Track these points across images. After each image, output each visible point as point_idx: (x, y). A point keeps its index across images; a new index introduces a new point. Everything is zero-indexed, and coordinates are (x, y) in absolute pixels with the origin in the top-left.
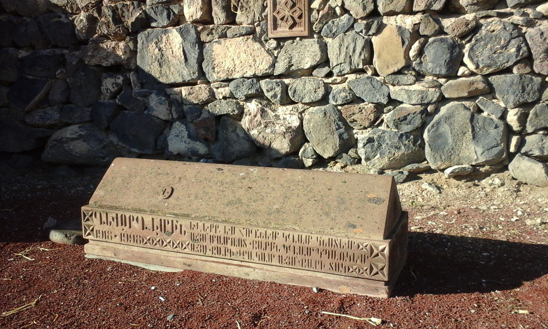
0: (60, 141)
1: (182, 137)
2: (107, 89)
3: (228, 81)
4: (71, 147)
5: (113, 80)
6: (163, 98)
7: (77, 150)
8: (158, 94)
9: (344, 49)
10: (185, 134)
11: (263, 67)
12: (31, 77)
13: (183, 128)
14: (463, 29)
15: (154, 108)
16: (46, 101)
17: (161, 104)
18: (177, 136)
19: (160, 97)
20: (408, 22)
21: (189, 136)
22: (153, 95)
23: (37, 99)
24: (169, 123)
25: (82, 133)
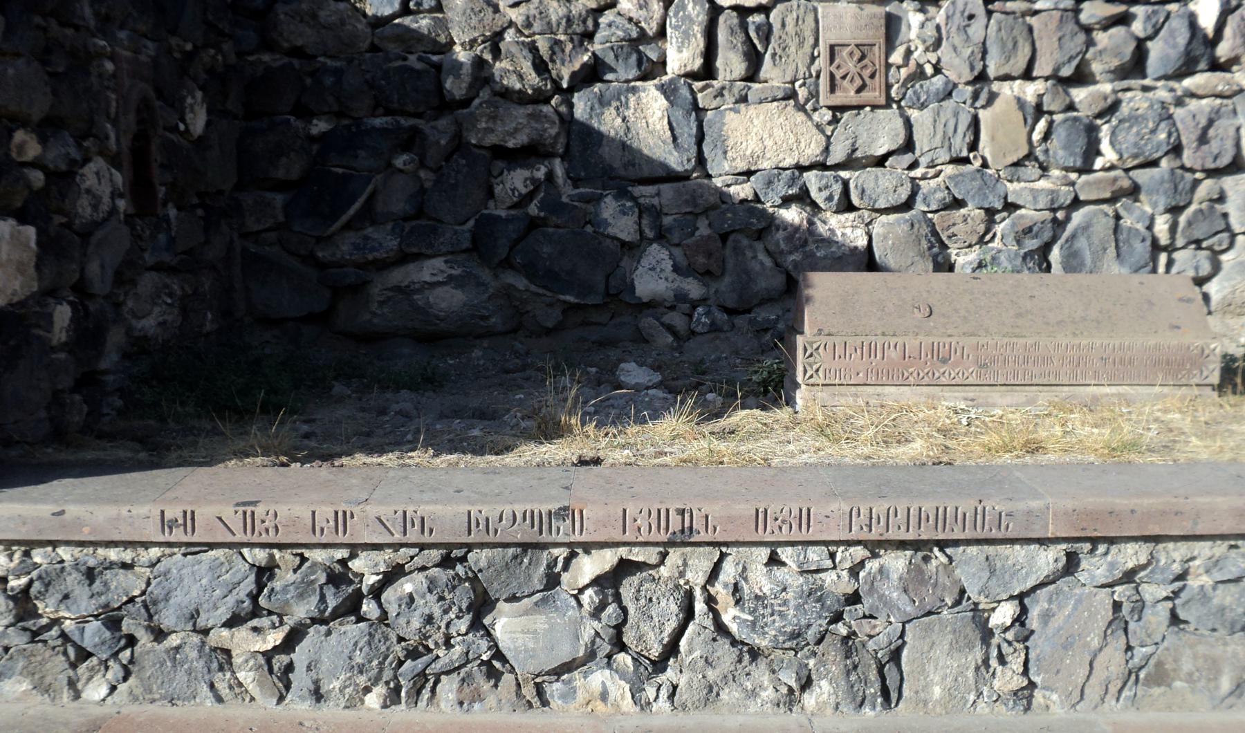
0: (405, 291)
1: (662, 270)
2: (513, 190)
3: (749, 174)
4: (431, 299)
5: (526, 173)
6: (629, 204)
7: (443, 305)
8: (617, 197)
9: (940, 128)
10: (668, 265)
11: (811, 150)
12: (340, 171)
13: (664, 254)
14: (1101, 105)
15: (610, 220)
16: (368, 215)
17: (625, 214)
18: (653, 269)
19: (623, 202)
20: (1030, 91)
21: (676, 269)
22: (608, 200)
23: (352, 211)
24: (632, 249)
25: (453, 272)
